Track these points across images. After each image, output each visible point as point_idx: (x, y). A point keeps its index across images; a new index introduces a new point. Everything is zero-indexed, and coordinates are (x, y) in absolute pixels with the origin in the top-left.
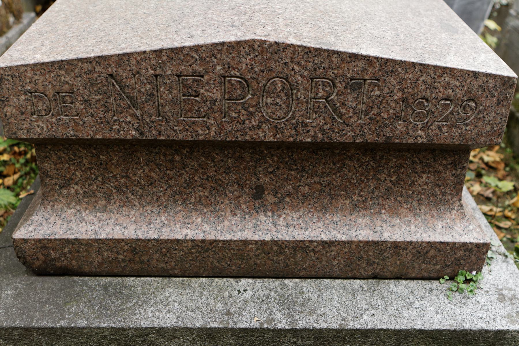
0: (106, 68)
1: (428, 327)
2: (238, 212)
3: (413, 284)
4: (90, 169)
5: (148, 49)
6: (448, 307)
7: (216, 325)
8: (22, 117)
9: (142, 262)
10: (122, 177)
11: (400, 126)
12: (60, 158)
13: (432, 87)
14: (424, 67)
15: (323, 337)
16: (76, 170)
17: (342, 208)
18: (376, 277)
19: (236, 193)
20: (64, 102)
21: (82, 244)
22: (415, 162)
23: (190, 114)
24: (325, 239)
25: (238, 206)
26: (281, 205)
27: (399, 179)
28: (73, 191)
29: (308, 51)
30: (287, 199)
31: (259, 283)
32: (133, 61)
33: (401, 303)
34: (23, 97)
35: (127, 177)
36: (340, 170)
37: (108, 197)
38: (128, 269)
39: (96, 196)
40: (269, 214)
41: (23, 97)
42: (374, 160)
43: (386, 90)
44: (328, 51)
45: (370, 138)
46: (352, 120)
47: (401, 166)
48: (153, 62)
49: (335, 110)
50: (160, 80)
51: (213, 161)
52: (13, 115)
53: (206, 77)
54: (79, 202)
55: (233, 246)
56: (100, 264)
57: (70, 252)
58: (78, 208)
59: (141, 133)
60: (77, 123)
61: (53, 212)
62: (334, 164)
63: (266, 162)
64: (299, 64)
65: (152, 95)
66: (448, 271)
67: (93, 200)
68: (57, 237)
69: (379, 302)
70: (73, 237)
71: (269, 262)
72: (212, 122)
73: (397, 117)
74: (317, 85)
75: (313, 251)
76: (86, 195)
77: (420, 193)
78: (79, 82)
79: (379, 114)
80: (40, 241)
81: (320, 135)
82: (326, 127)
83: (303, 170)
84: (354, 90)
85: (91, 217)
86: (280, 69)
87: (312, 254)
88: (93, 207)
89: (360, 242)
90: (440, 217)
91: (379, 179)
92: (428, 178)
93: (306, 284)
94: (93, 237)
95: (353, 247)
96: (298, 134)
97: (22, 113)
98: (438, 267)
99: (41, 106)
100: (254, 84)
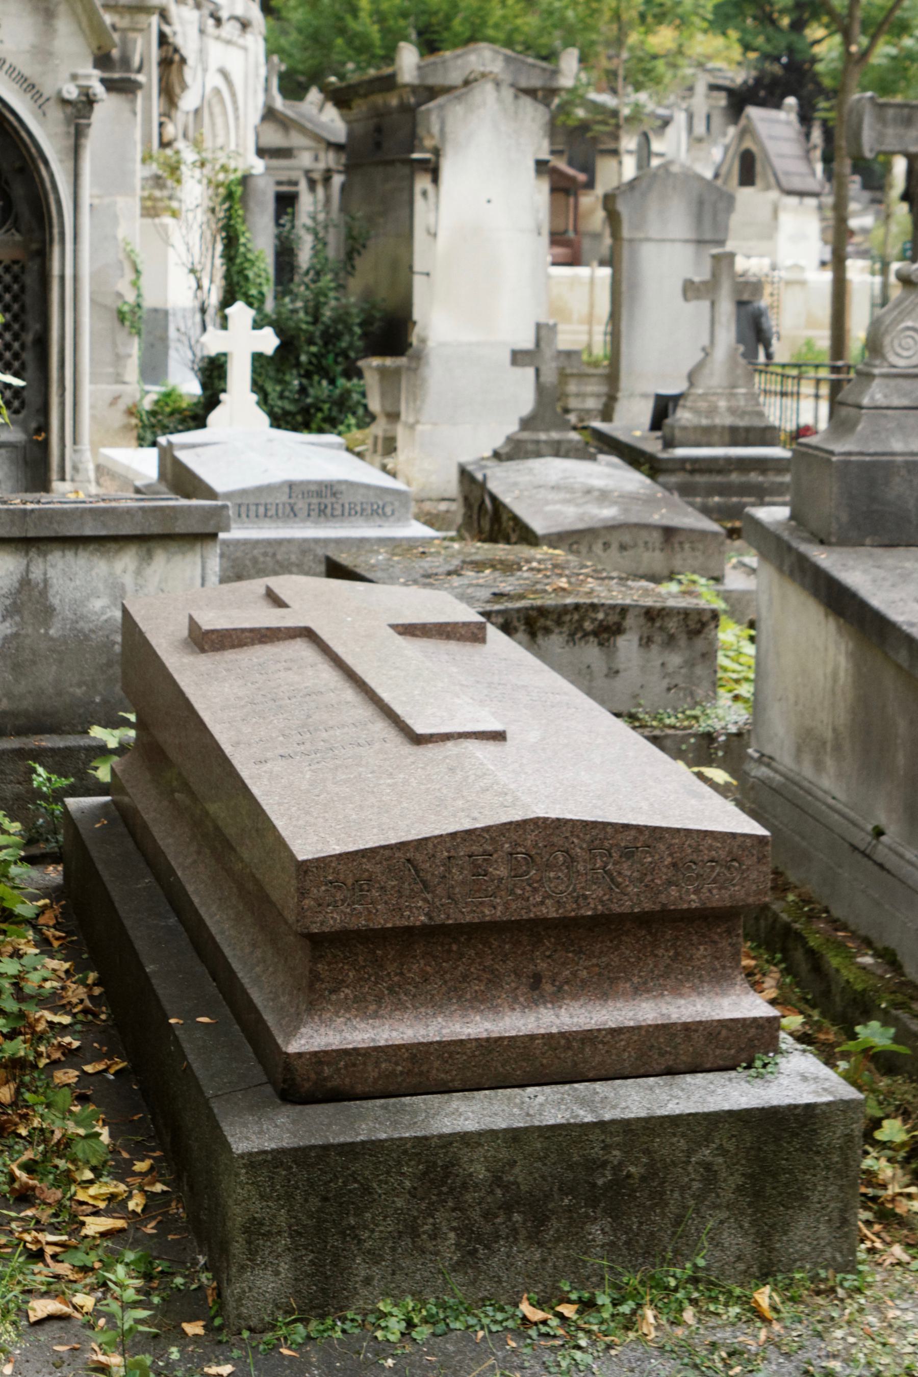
0: (404, 854)
1: (735, 1107)
2: (517, 1006)
3: (710, 1076)
4: (364, 967)
5: (444, 833)
6: (753, 1091)
7: (521, 1125)
8: (319, 909)
9: (421, 1073)
10: (396, 975)
11: (674, 891)
12: (335, 956)
13: (697, 850)
14: (688, 832)
15: (631, 1130)
16: (349, 970)
17: (623, 994)
18: (671, 1072)
19: (513, 985)
20: (361, 890)
21: (359, 1054)
22: (690, 933)
23: (478, 895)
24: (614, 1026)
25: (516, 999)
26: (560, 995)
27: (677, 954)
28: (342, 995)
29: (585, 824)
30: (566, 987)
31: (547, 1089)
32: (430, 845)
33: (703, 1092)
34: (323, 888)
35: (402, 974)
36: (617, 948)
37: (379, 1000)
38: (404, 1085)
39: (366, 1001)
40: (549, 1005)
41: (323, 888)
42: (650, 933)
43: (657, 857)
44: (602, 823)
45: (648, 906)
46: (629, 889)
47: (677, 938)
48: (448, 845)
49: (612, 880)
50: (452, 861)
51: (490, 948)
52: (310, 908)
53: (495, 856)
54: (348, 1010)
55: (519, 1044)
56: (376, 1081)
57: (346, 1066)
58: (348, 1016)
59: (431, 918)
60: (370, 912)
61: (322, 1022)
62: (611, 941)
63: (544, 944)
64: (578, 837)
65: (444, 877)
66: (744, 1056)
67: (363, 1004)
68: (334, 1047)
69: (680, 1093)
70: (351, 1046)
71: (556, 1061)
72: (498, 900)
73: (670, 883)
74: (595, 856)
75: (602, 1042)
76: (356, 1000)
77: (699, 969)
78: (378, 869)
79: (653, 880)
80: (315, 1054)
81: (600, 907)
82: (605, 898)
83: (581, 952)
84: (628, 859)
85: (363, 1025)
86: (561, 843)
87: (600, 1046)
88: (365, 1016)
89: (650, 1026)
90: (724, 994)
91: (656, 956)
92: (706, 949)
93: (598, 1086)
94: (372, 1045)
95: (643, 1033)
96: (579, 908)
97: (320, 905)
98: (733, 1052)
99: (339, 896)
100: (538, 859)
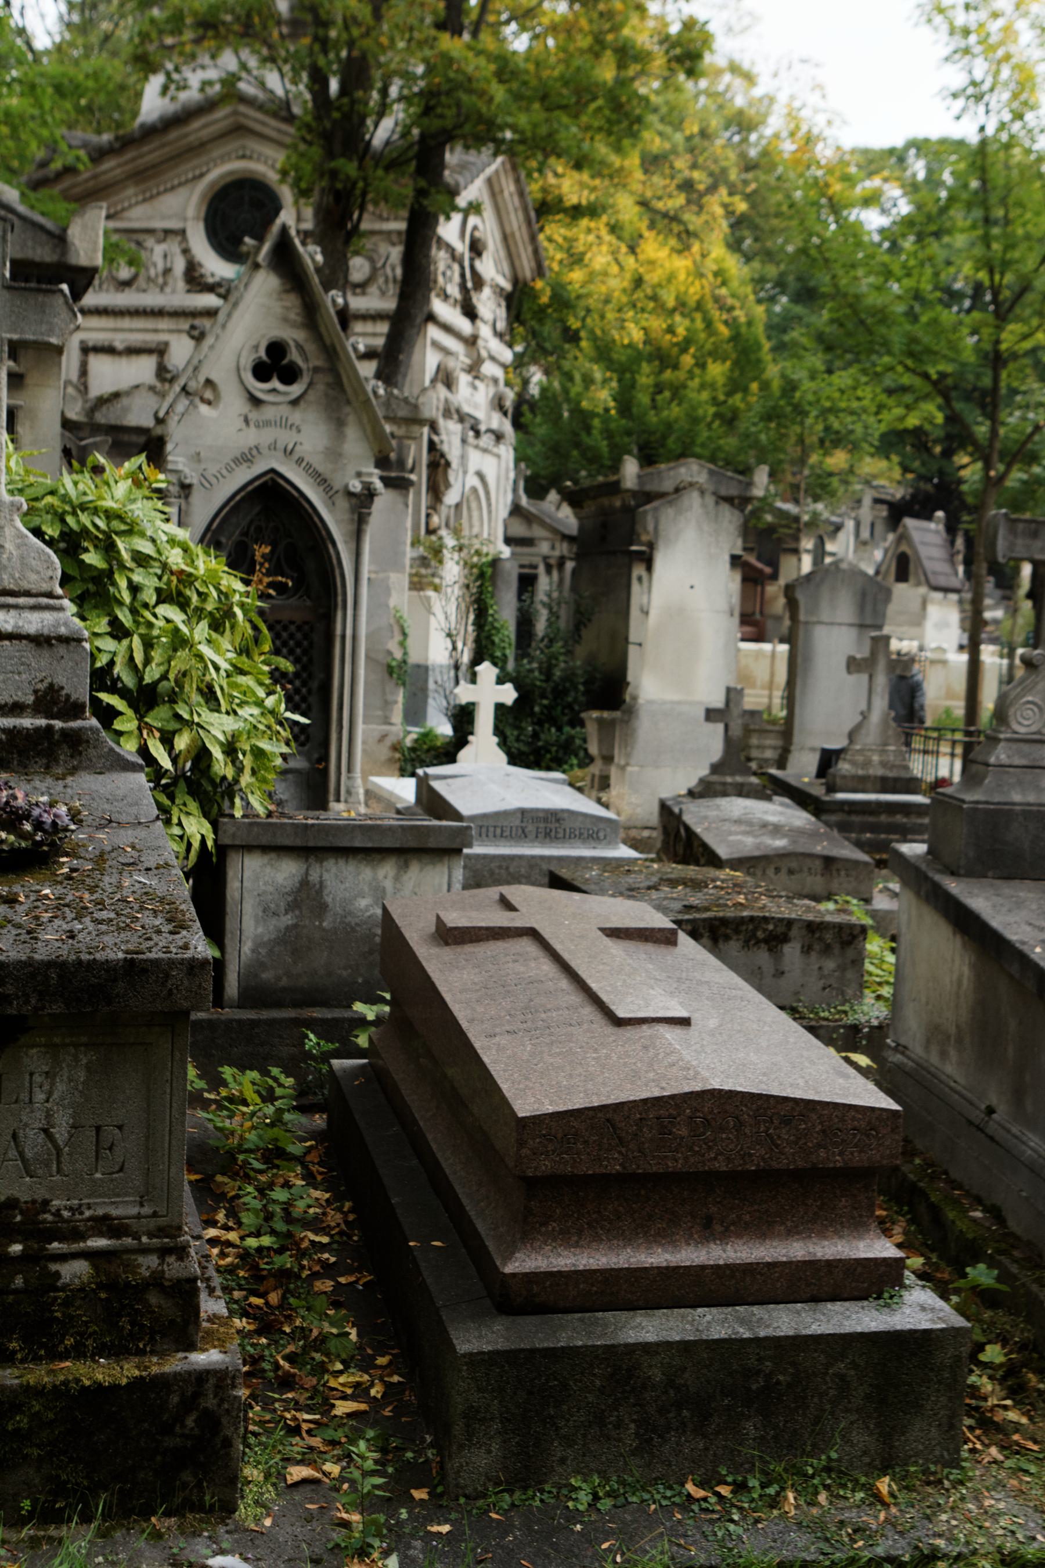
3: (847, 1304)
11: (822, 1153)
13: (842, 1120)
14: (836, 1105)
25: (691, 1236)
31: (714, 1310)
37: (580, 1233)
45: (801, 1164)
54: (554, 1240)
73: (819, 1146)
90: (861, 1238)
93: (755, 1309)
99: (550, 1147)
